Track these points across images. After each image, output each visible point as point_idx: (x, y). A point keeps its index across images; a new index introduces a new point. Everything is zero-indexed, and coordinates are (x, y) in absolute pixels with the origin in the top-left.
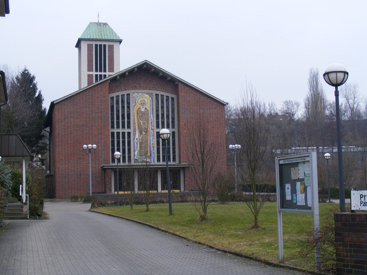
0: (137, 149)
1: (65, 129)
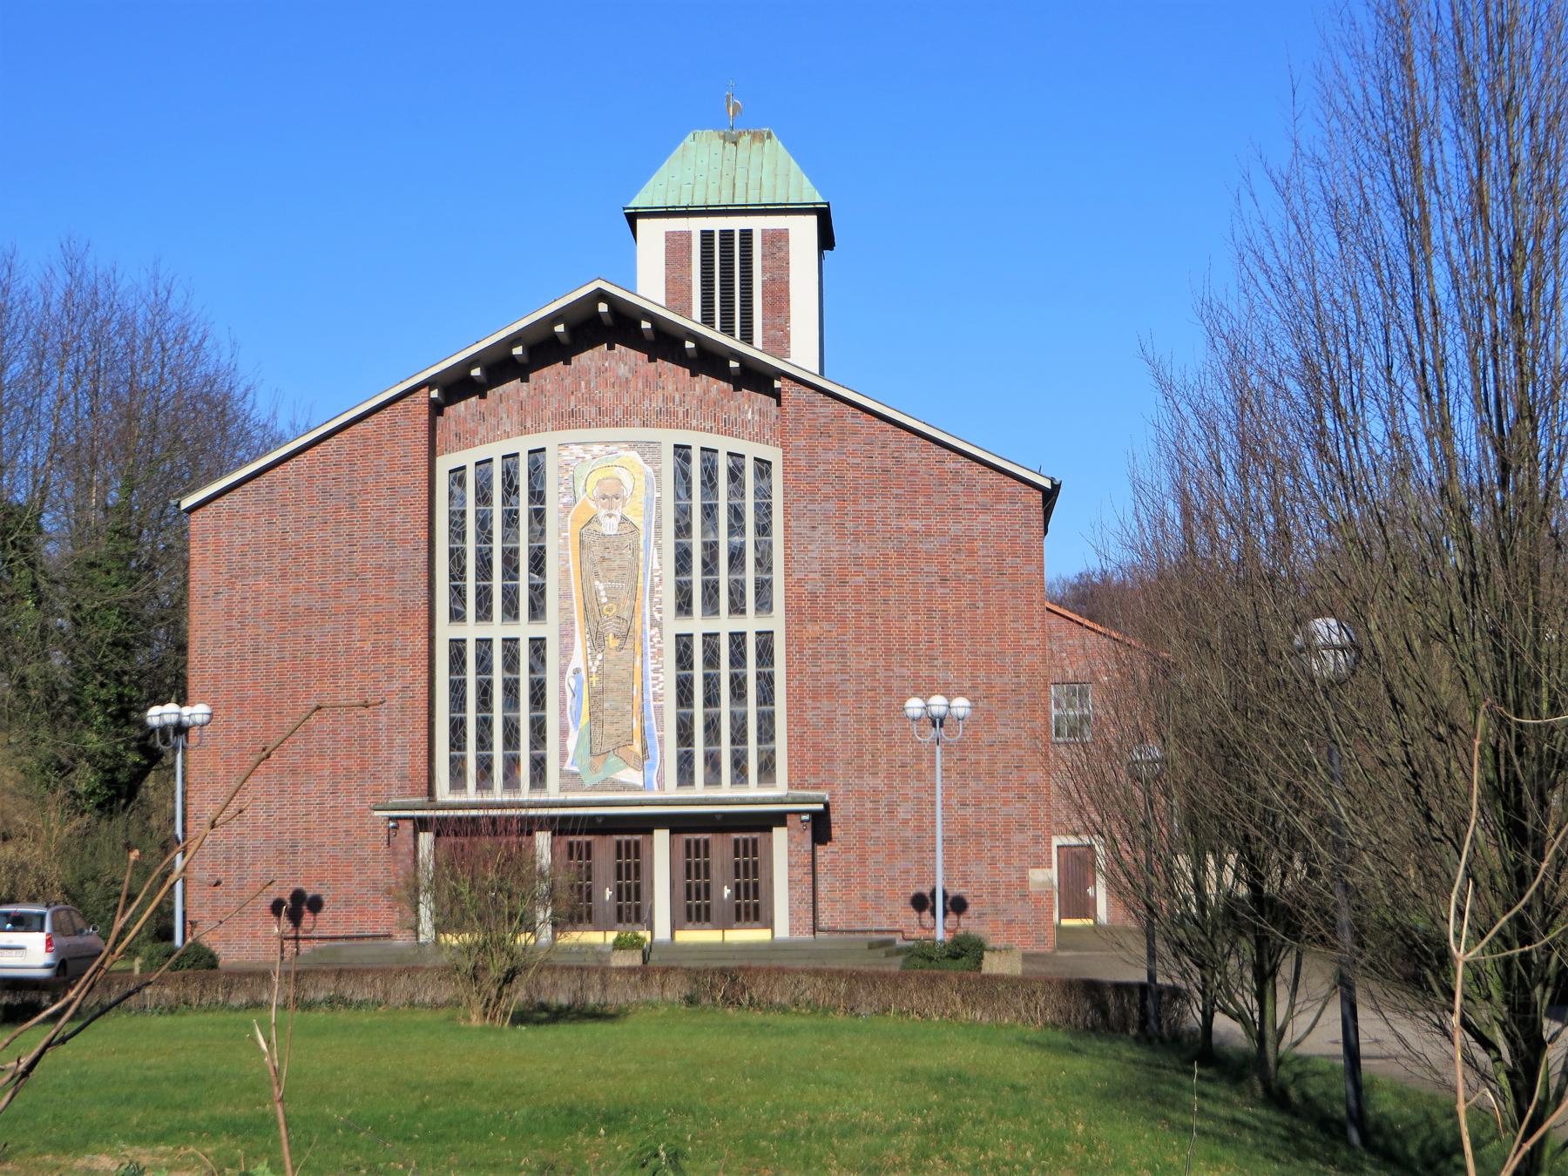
0: (576, 723)
1: (230, 629)
